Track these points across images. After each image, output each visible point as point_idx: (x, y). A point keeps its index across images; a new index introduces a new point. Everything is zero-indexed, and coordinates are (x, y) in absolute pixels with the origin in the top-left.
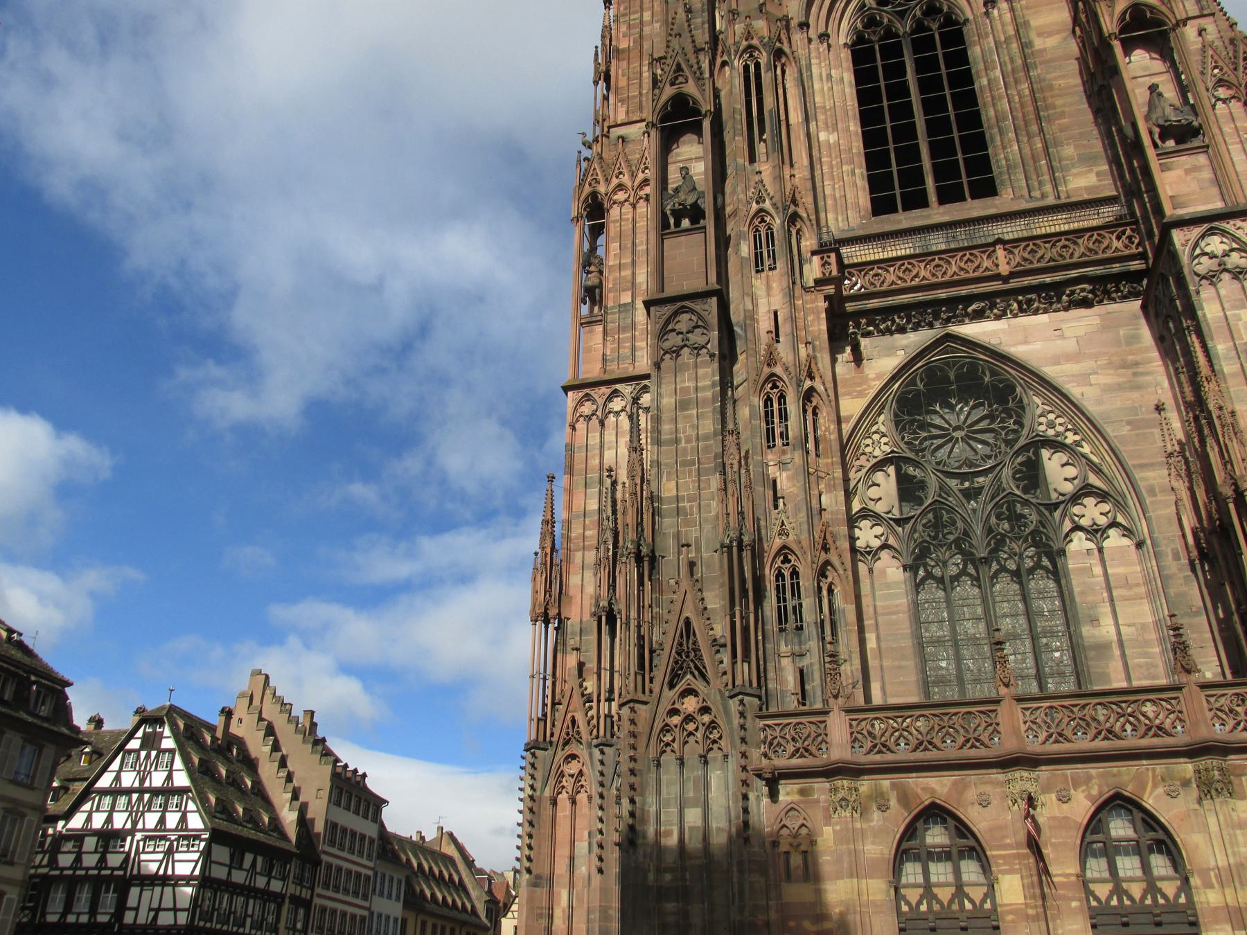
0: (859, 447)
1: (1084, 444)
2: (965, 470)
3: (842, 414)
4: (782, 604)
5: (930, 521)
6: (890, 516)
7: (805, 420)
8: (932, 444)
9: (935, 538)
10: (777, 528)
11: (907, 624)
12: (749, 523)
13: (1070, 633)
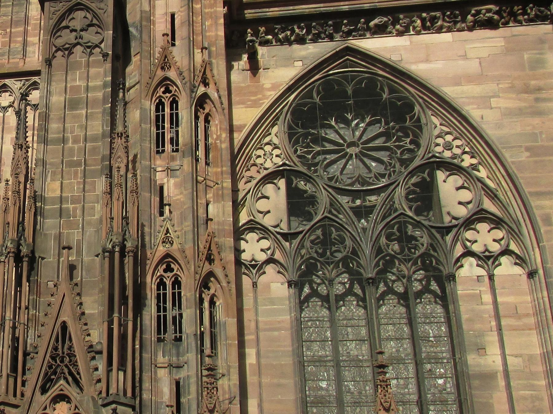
0: (250, 158)
1: (481, 168)
2: (357, 187)
3: (235, 123)
4: (162, 314)
5: (318, 237)
6: (278, 230)
7: (197, 127)
8: (325, 159)
9: (323, 255)
10: (161, 236)
11: (288, 342)
12: (133, 229)
13: (455, 360)
